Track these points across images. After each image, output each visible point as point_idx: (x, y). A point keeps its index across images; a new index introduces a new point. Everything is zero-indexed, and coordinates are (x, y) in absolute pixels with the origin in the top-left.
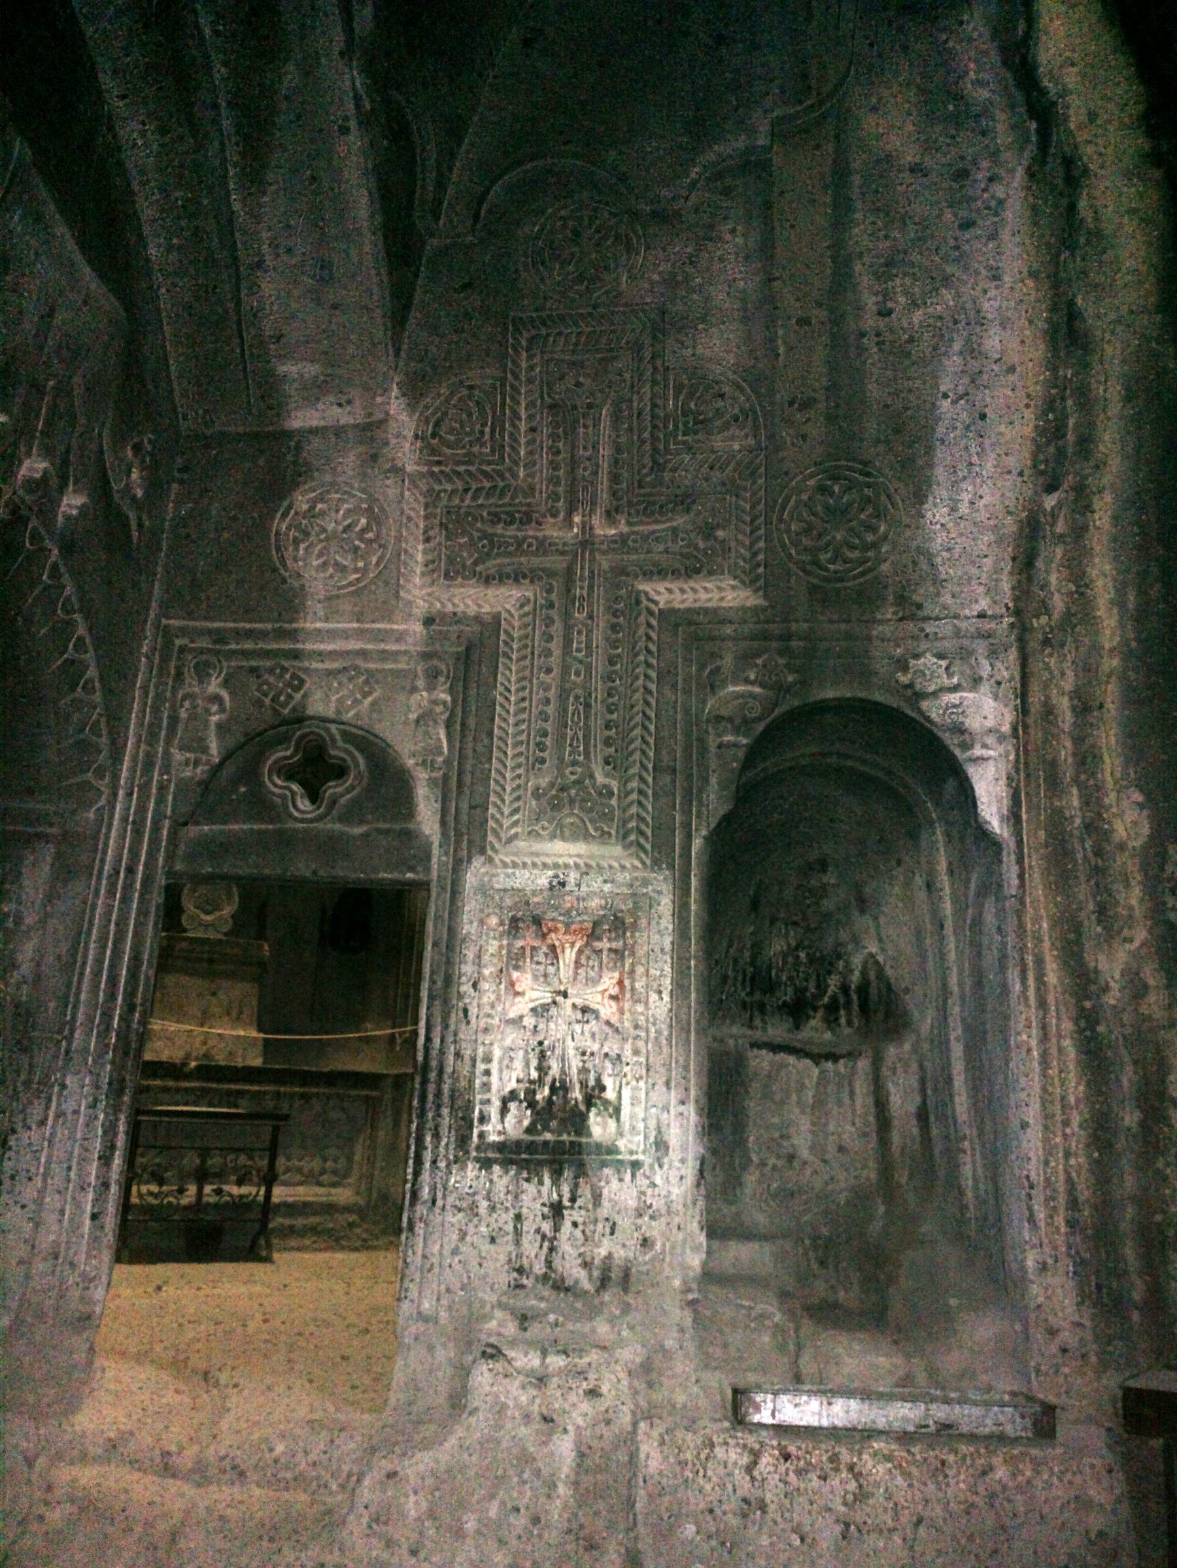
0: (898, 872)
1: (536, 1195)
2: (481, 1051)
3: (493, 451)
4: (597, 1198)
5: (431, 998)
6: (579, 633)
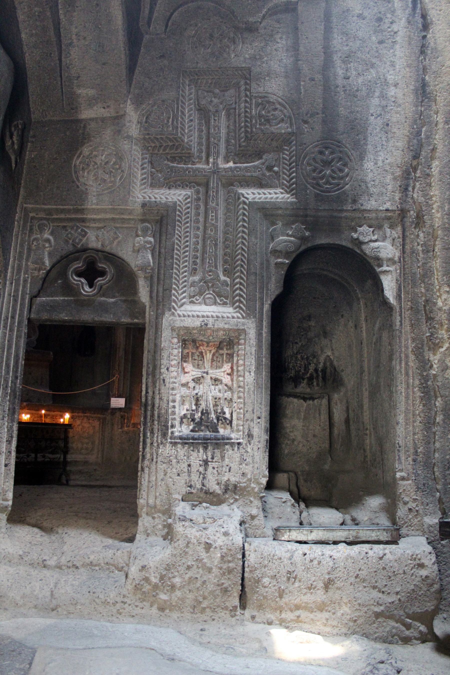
0: (342, 321)
1: (197, 457)
2: (171, 398)
3: (173, 129)
4: (223, 458)
5: (148, 374)
6: (212, 212)
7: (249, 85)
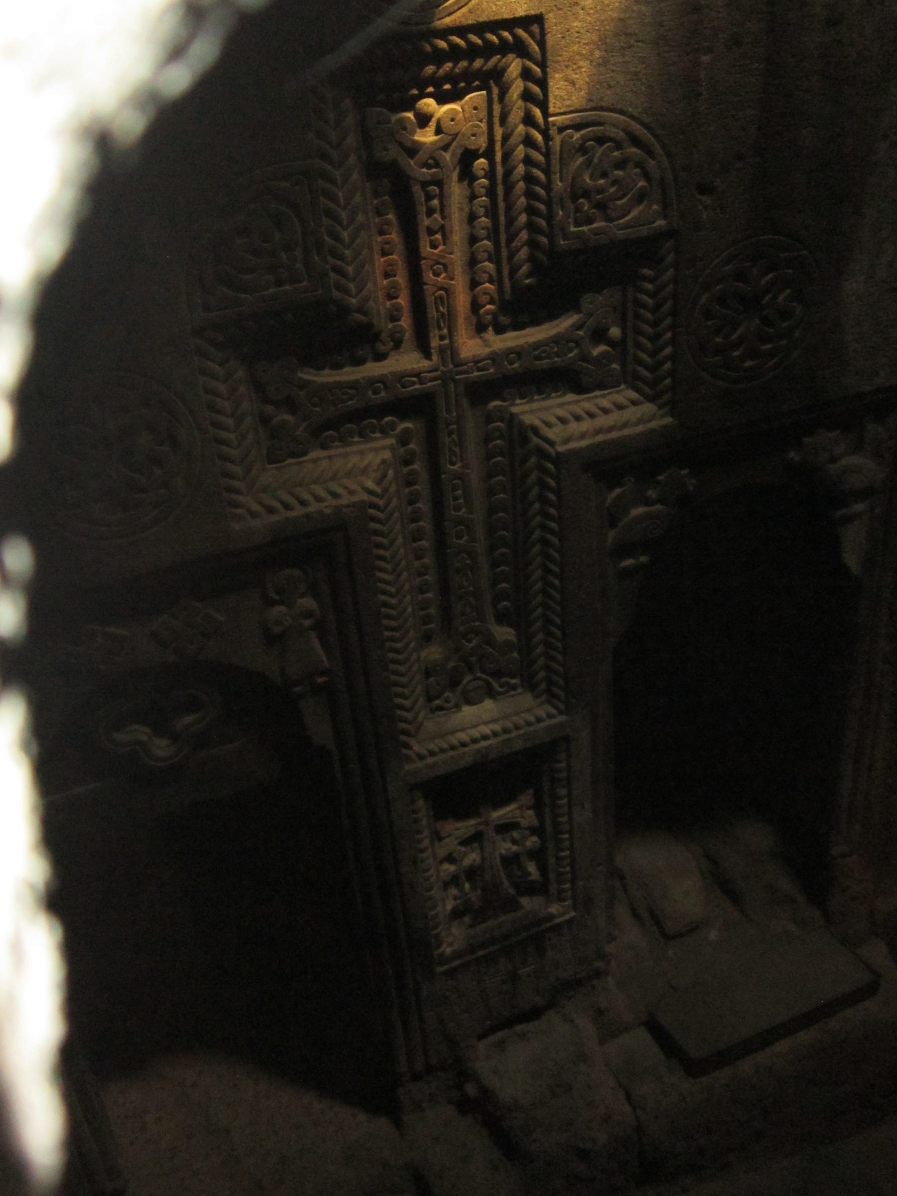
7: (543, 83)
